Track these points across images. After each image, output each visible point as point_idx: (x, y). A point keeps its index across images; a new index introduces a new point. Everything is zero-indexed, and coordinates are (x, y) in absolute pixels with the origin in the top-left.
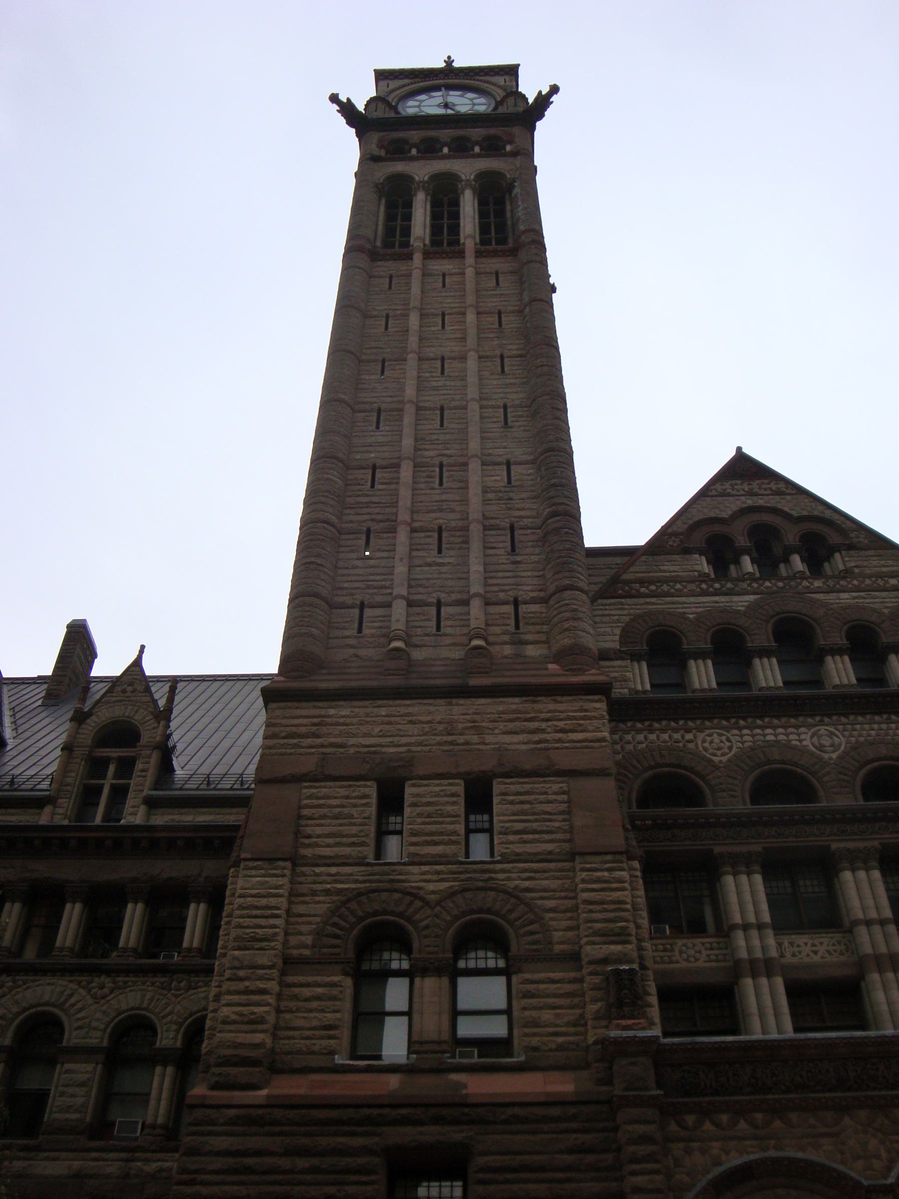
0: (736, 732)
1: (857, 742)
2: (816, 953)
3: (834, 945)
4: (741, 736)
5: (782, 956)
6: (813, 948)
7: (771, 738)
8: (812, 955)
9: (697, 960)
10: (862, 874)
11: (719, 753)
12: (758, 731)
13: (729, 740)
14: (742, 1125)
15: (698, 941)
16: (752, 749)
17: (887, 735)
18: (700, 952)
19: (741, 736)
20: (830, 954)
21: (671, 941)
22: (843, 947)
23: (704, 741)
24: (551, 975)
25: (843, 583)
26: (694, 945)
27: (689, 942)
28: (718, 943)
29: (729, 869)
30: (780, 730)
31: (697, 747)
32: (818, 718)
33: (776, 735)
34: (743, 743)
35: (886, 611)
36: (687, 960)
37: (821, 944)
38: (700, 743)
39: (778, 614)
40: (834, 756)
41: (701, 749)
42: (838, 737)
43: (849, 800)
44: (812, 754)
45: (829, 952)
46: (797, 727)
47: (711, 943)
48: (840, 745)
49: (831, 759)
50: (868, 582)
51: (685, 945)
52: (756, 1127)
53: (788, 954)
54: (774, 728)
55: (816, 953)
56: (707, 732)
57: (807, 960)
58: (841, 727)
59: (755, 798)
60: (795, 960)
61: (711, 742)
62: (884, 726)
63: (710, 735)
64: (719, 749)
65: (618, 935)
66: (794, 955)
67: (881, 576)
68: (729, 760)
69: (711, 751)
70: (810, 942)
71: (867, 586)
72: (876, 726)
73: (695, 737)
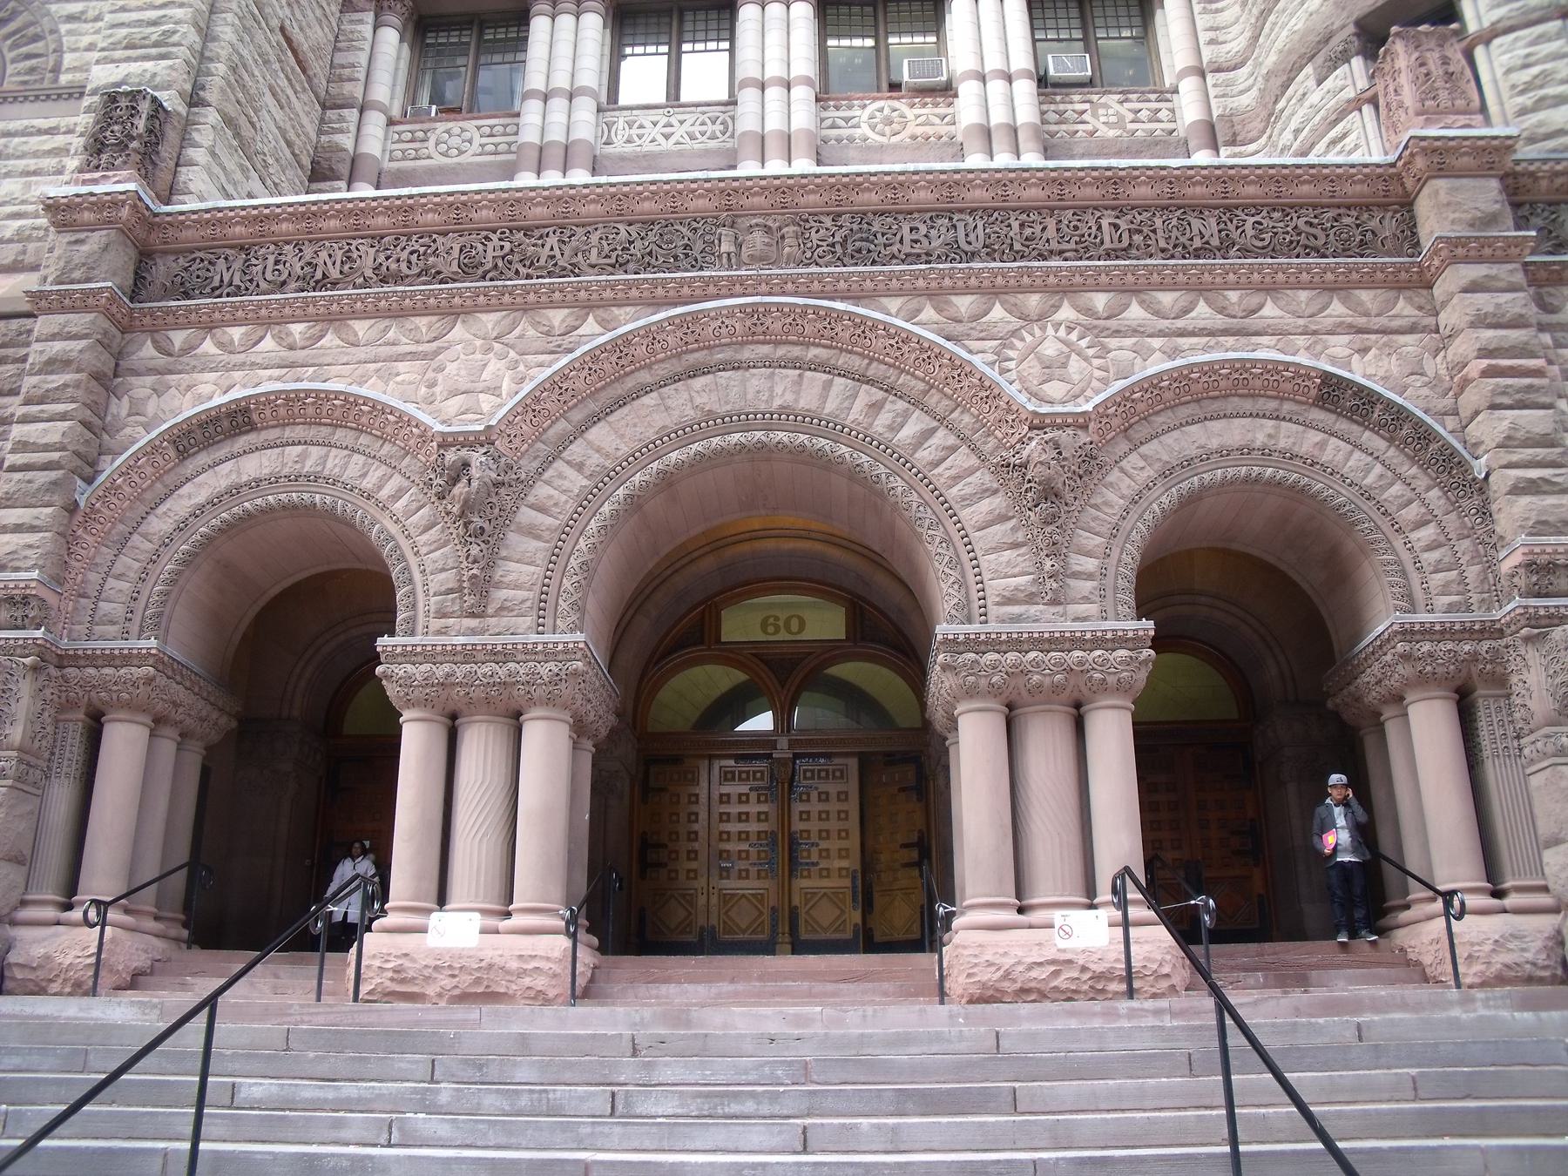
2: (667, 137)
9: (461, 152)
14: (268, 343)
15: (470, 125)
18: (470, 141)
21: (426, 126)
22: (718, 127)
24: (43, 123)
26: (463, 130)
27: (455, 126)
28: (506, 126)
29: (547, 8)
36: (445, 154)
37: (681, 122)
45: (693, 138)
47: (492, 127)
51: (447, 131)
52: (291, 348)
55: (667, 137)
60: (629, 148)
65: (156, 45)
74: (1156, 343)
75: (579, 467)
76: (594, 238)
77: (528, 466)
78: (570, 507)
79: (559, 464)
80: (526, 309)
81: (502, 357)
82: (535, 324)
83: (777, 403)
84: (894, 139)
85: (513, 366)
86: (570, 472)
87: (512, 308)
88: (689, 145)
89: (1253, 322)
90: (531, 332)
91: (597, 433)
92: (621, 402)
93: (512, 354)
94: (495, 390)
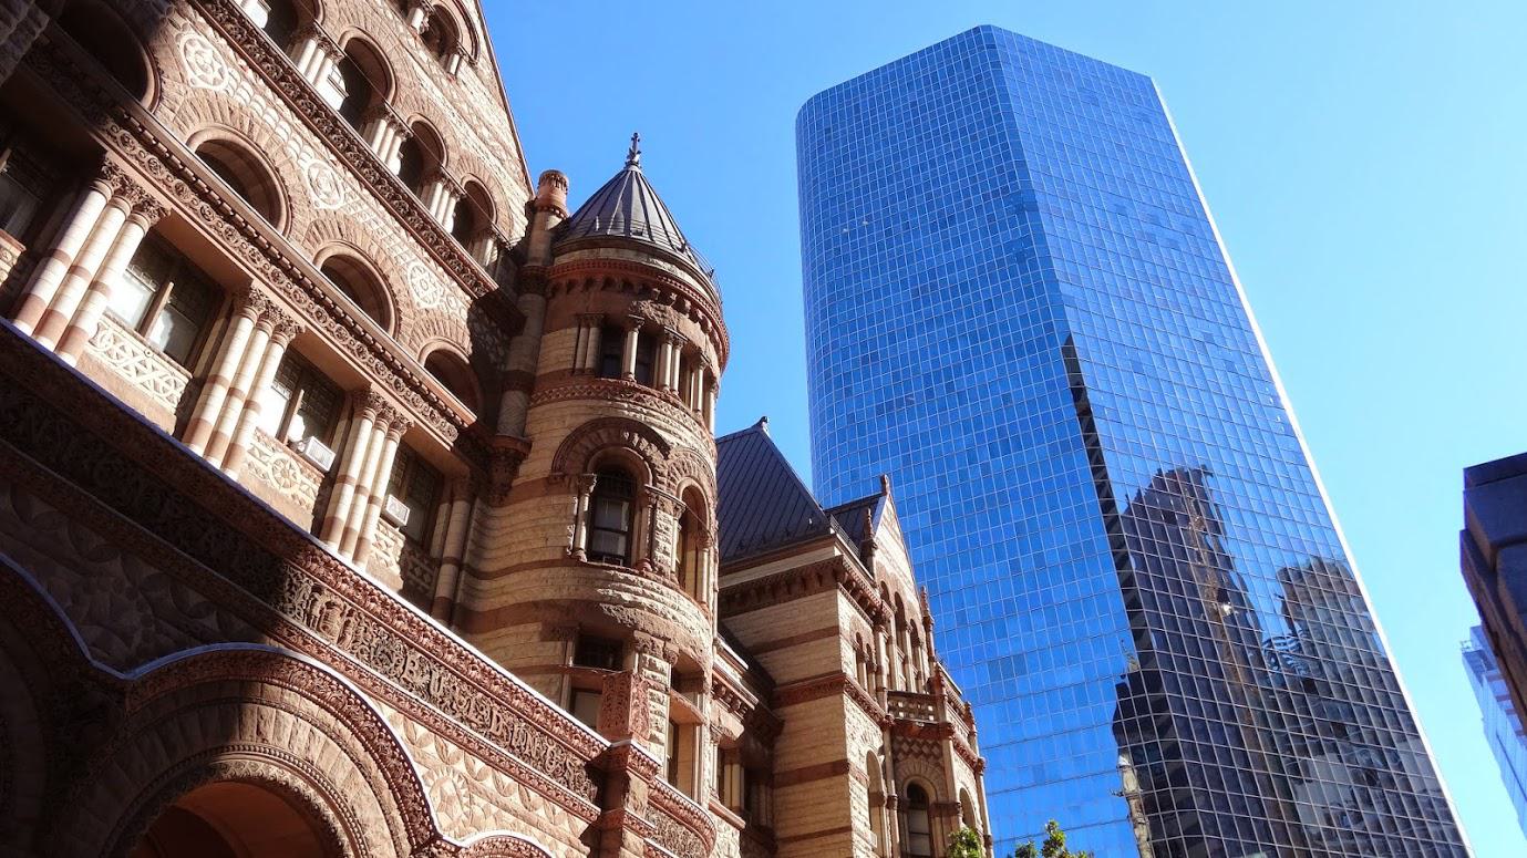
3: (167, 382)
6: (141, 367)
11: (200, 72)
20: (155, 388)
23: (190, 41)
43: (306, 253)
53: (102, 346)
56: (203, 39)
57: (123, 373)
59: (202, 153)
60: (105, 361)
64: (202, 68)
69: (191, 59)
70: (141, 357)
74: (494, 809)
84: (283, 491)
88: (151, 393)
89: (533, 815)
90: (170, 601)
93: (150, 612)
94: (126, 638)
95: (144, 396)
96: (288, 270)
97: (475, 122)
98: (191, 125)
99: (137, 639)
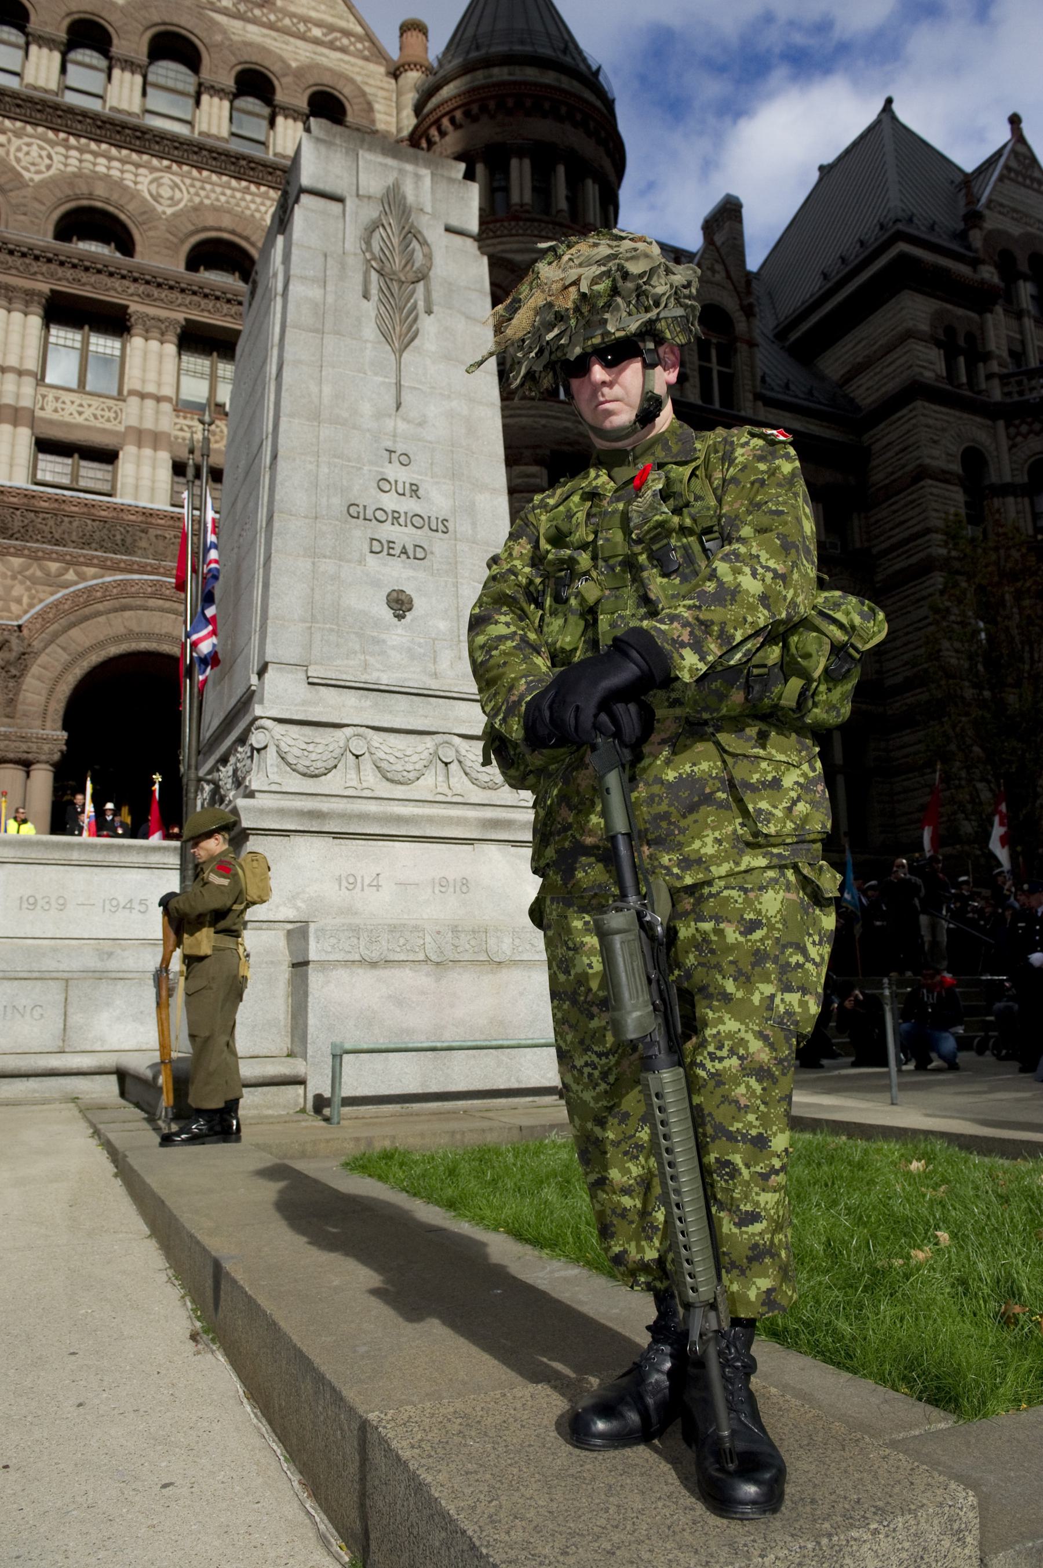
0: (62, 150)
1: (201, 203)
2: (80, 413)
4: (67, 157)
5: (42, 409)
7: (104, 170)
8: (76, 415)
10: (154, 344)
11: (33, 169)
12: (88, 157)
13: (50, 157)
16: (75, 175)
17: (238, 205)
19: (67, 157)
22: (112, 415)
23: (19, 149)
25: (257, 12)
30: (115, 164)
31: (8, 153)
32: (166, 163)
33: (109, 168)
34: (66, 165)
35: (294, 64)
38: (12, 150)
39: (164, 24)
40: (169, 211)
41: (12, 157)
42: (181, 190)
44: (144, 201)
45: (95, 417)
46: (138, 166)
48: (181, 200)
49: (164, 213)
50: (287, 21)
53: (49, 408)
54: (110, 159)
55: (80, 413)
56: (27, 140)
57: (68, 419)
58: (188, 181)
60: (55, 416)
61: (27, 153)
62: (238, 195)
63: (29, 145)
64: (33, 164)
66: (56, 411)
67: (306, 20)
68: (42, 181)
69: (23, 164)
71: (286, 26)
72: (228, 192)
73: (9, 141)
75: (64, 649)
76: (75, 524)
77: (36, 644)
78: (59, 668)
79: (53, 646)
80: (37, 559)
81: (22, 583)
82: (41, 568)
83: (163, 631)
85: (28, 589)
86: (60, 651)
87: (29, 557)
88: (94, 423)
90: (39, 573)
91: (74, 632)
92: (87, 618)
93: (28, 583)
94: (19, 601)
95: (89, 428)
96: (156, 282)
97: (302, 27)
98: (40, 215)
99: (25, 600)
